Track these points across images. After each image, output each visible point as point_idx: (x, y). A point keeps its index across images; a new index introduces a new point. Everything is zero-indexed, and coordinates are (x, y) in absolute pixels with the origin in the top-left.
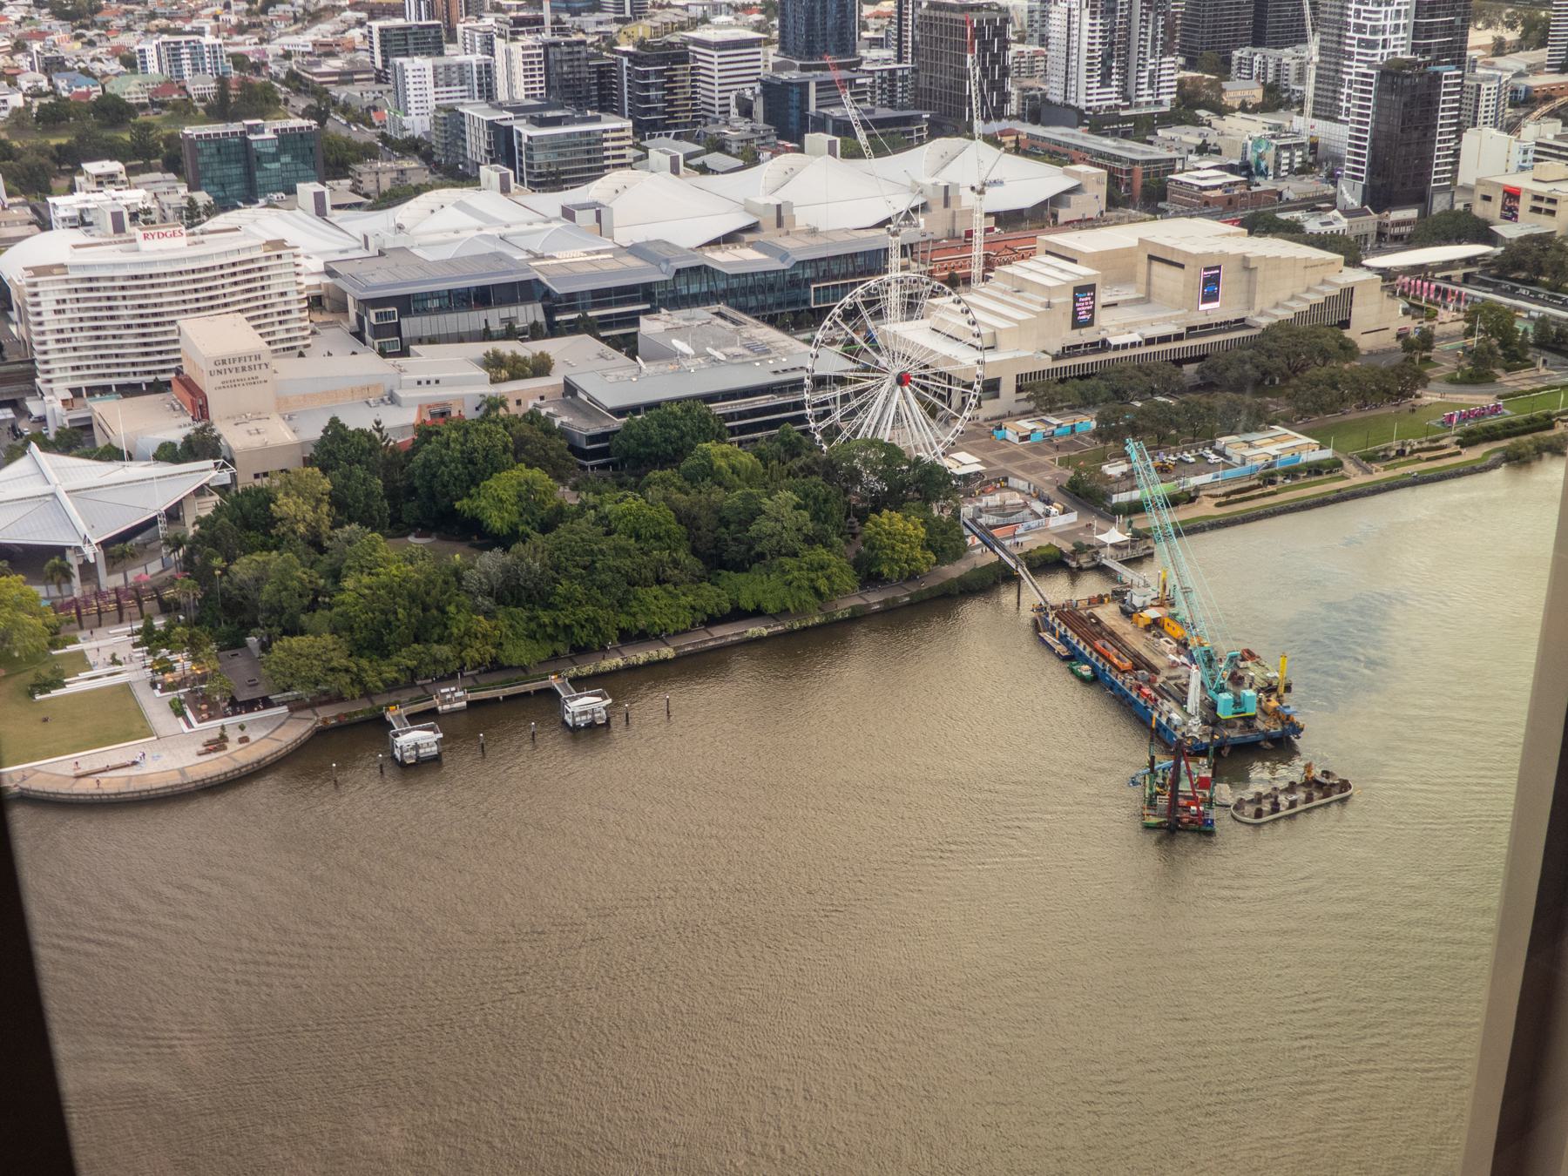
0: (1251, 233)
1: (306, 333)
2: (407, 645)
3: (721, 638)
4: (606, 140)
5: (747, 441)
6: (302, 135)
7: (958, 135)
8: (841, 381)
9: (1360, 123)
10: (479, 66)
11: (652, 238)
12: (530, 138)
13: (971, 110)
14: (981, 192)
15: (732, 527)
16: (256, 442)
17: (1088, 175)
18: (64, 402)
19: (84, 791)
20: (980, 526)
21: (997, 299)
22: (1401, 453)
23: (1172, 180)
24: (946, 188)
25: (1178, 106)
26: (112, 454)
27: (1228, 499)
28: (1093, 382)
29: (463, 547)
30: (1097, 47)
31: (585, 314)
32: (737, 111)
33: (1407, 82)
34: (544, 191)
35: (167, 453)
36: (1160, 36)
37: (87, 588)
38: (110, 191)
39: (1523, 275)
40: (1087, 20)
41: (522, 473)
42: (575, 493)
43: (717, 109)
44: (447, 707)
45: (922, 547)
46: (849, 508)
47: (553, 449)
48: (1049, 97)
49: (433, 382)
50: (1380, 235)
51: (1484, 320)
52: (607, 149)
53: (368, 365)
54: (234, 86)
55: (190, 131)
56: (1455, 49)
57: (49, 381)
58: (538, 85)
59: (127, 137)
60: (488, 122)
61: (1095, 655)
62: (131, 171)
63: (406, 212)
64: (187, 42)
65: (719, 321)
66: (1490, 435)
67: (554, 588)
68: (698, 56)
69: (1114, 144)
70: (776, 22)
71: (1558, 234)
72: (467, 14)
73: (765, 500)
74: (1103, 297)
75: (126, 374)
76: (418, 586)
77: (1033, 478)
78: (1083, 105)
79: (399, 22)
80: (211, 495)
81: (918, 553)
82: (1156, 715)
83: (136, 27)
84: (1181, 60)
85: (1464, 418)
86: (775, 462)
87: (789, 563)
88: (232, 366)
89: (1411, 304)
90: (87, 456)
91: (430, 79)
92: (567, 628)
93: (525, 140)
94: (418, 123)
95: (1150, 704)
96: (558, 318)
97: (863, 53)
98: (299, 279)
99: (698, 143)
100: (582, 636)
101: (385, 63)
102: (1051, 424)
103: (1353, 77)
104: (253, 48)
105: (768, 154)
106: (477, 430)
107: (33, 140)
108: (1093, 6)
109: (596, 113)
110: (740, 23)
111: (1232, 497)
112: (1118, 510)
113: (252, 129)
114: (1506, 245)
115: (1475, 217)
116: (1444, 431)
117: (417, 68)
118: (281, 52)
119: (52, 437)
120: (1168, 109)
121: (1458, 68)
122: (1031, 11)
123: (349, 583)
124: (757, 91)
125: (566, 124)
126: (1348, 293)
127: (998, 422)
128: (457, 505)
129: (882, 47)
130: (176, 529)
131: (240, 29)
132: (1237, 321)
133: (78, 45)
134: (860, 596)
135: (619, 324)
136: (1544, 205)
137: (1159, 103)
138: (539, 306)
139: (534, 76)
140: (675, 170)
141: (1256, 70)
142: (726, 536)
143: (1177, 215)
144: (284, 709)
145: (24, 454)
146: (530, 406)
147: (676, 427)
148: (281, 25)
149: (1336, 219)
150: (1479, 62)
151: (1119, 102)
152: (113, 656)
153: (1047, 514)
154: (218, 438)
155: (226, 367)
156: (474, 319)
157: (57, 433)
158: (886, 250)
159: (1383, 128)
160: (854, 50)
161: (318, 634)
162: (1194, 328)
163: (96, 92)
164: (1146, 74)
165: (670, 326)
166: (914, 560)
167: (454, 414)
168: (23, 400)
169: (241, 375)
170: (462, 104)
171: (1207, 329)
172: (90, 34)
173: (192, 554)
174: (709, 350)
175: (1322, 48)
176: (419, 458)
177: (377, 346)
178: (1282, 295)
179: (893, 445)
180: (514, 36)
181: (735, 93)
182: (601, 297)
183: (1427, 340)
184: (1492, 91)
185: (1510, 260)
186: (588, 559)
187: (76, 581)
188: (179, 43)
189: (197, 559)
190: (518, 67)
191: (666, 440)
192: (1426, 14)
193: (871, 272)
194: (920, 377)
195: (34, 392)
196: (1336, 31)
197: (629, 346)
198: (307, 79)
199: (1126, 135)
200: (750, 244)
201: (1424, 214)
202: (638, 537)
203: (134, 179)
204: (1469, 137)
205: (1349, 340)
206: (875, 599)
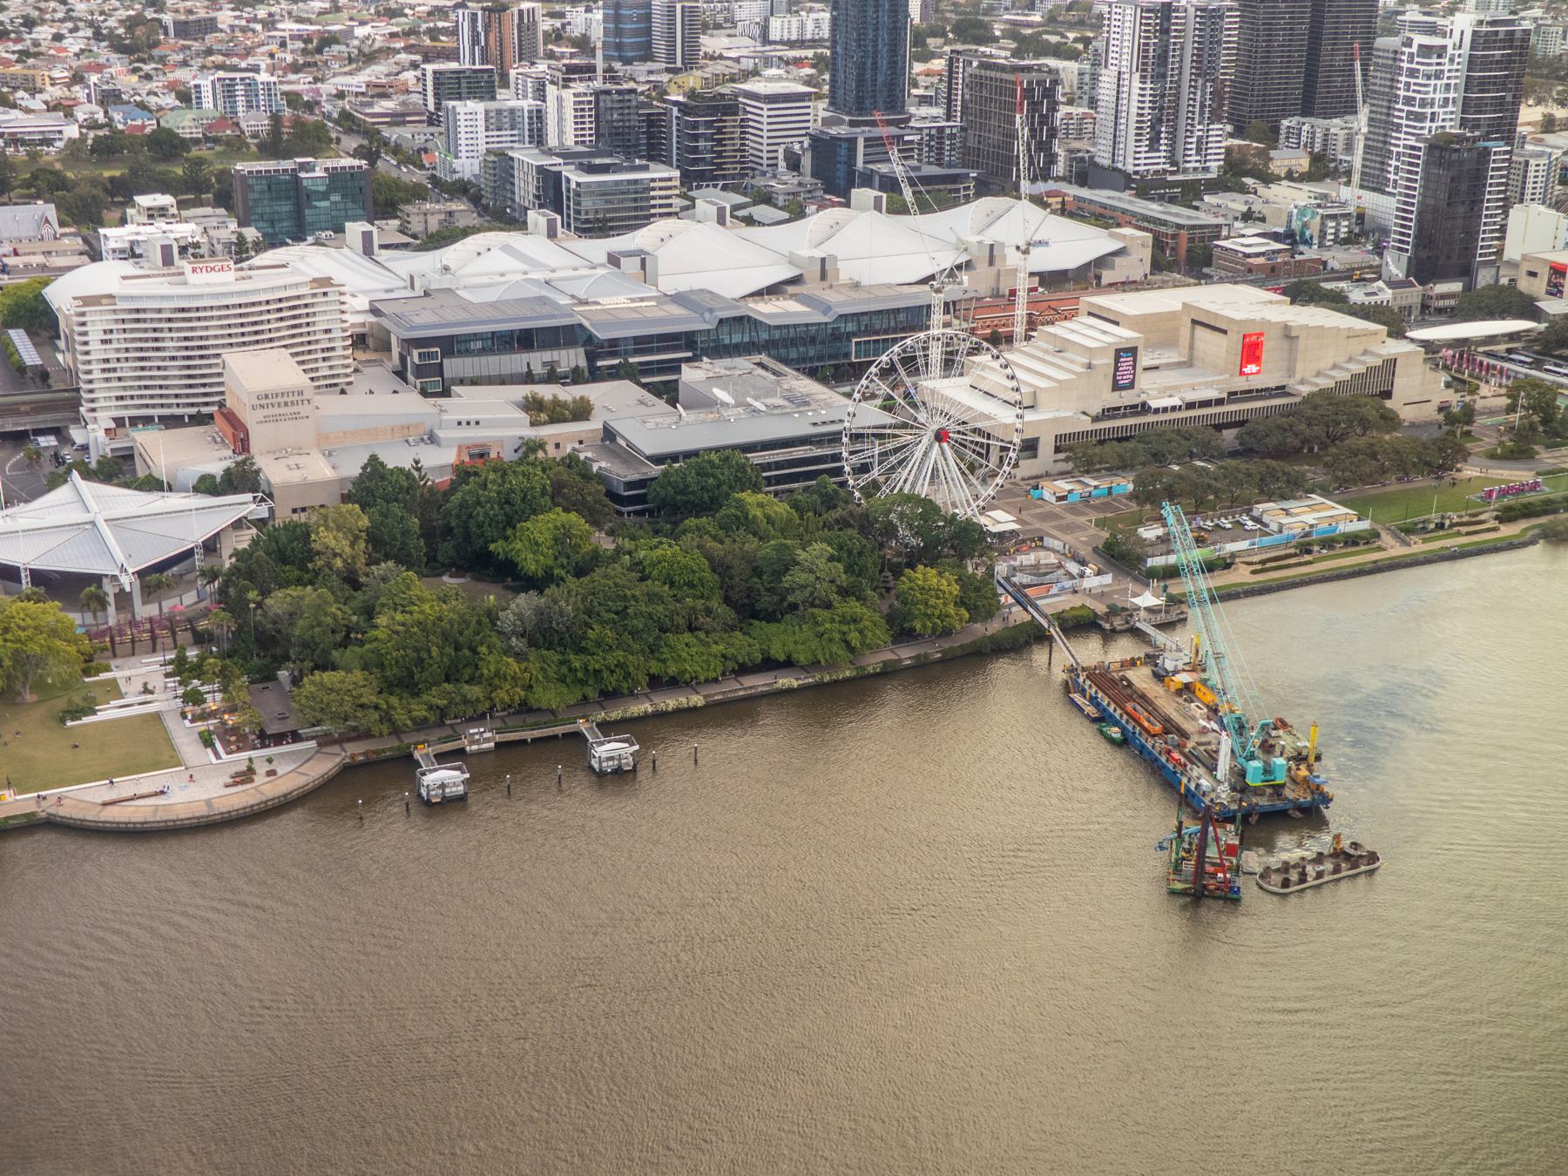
0: (1292, 303)
1: (349, 371)
2: (437, 684)
3: (751, 688)
4: (653, 189)
5: (783, 492)
6: (352, 175)
7: (1005, 195)
9: (1407, 195)
10: (530, 112)
11: (696, 287)
12: (578, 184)
13: (1018, 170)
14: (1026, 252)
15: (765, 577)
16: (295, 477)
17: (1133, 238)
18: (107, 431)
19: (111, 819)
20: (1014, 585)
21: (1039, 359)
22: (1440, 526)
23: (1218, 246)
24: (992, 246)
25: (1226, 173)
26: (153, 484)
27: (1263, 566)
28: (1131, 445)
29: (498, 588)
30: (1147, 111)
31: (626, 360)
32: (784, 164)
33: (1455, 156)
34: (591, 238)
35: (207, 486)
36: (1208, 103)
38: (161, 224)
40: (1136, 84)
41: (558, 517)
42: (612, 539)
43: (765, 162)
44: (475, 747)
45: (956, 603)
46: (883, 564)
47: (590, 494)
48: (1096, 159)
49: (473, 423)
50: (1425, 307)
51: (1528, 396)
52: (654, 198)
53: (410, 404)
54: (287, 124)
56: (1505, 125)
57: (93, 410)
58: (588, 132)
59: (179, 171)
60: (537, 167)
61: (1125, 717)
62: (182, 205)
63: (452, 254)
64: (242, 79)
65: (760, 371)
66: (1528, 512)
67: (585, 633)
68: (748, 109)
69: (1161, 208)
70: (827, 77)
72: (520, 60)
73: (799, 551)
74: (1145, 360)
75: (170, 406)
76: (452, 626)
77: (1068, 538)
78: (1130, 168)
79: (454, 65)
80: (249, 528)
81: (951, 610)
82: (1185, 780)
83: (192, 63)
84: (1229, 128)
85: (1504, 493)
86: (810, 514)
87: (822, 614)
88: (275, 400)
89: (1454, 378)
90: (127, 485)
91: (481, 123)
92: (597, 672)
93: (573, 186)
94: (467, 166)
95: (1179, 769)
96: (599, 364)
97: (912, 110)
98: (344, 317)
99: (745, 195)
100: (611, 681)
101: (438, 106)
102: (1087, 485)
103: (1401, 150)
104: (307, 86)
106: (514, 472)
108: (1143, 70)
109: (644, 162)
110: (791, 77)
111: (1268, 565)
112: (1153, 574)
113: (303, 167)
114: (1549, 322)
115: (1521, 293)
116: (1482, 506)
117: (469, 110)
118: (334, 92)
119: (93, 465)
120: (1215, 176)
121: (1507, 144)
122: (1081, 74)
123: (382, 620)
124: (806, 145)
126: (1391, 364)
127: (1035, 481)
128: (492, 547)
129: (931, 105)
130: (212, 561)
131: (295, 68)
132: (1277, 388)
133: (135, 78)
134: (892, 651)
137: (1206, 169)
138: (581, 351)
139: (584, 123)
140: (721, 221)
141: (1303, 139)
142: (759, 586)
143: (1221, 280)
144: (313, 744)
145: (66, 481)
146: (569, 450)
147: (713, 475)
149: (1381, 290)
150: (1529, 138)
151: (1167, 167)
152: (145, 684)
153: (1082, 575)
154: (257, 472)
155: (269, 401)
156: (516, 362)
157: (99, 462)
158: (929, 306)
159: (1432, 202)
160: (903, 107)
161: (349, 671)
162: (1235, 393)
164: (1194, 140)
165: (711, 375)
166: (948, 616)
167: (493, 455)
168: (67, 427)
169: (283, 410)
170: (512, 148)
171: (1249, 395)
172: (147, 68)
173: (228, 587)
174: (749, 400)
175: (1371, 119)
176: (456, 498)
177: (418, 385)
178: (1325, 364)
179: (930, 501)
180: (566, 84)
181: (783, 146)
182: (643, 344)
183: (1468, 414)
184: (1541, 168)
185: (1555, 337)
186: (620, 605)
187: (111, 610)
188: (234, 79)
189: (232, 591)
190: (569, 114)
191: (702, 488)
192: (1476, 89)
193: (914, 328)
194: (959, 432)
195: (78, 420)
196: (1385, 104)
197: (669, 393)
198: (360, 120)
199: (1172, 200)
200: (793, 296)
201: (1468, 288)
202: (672, 584)
203: (184, 213)
204: (1516, 212)
205: (1391, 411)
206: (906, 654)
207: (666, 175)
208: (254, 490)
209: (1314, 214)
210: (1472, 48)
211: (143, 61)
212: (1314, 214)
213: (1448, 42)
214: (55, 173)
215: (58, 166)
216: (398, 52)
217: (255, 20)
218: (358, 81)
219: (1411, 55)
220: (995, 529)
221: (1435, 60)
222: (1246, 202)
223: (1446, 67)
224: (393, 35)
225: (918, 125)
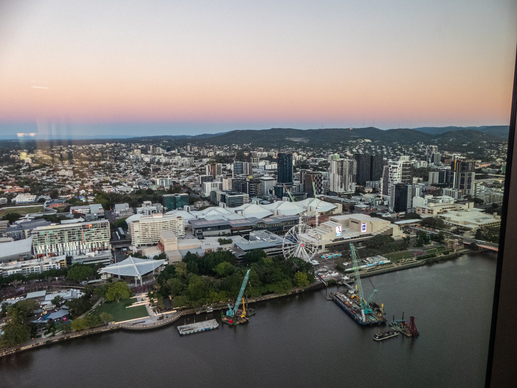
0: (371, 217)
2: (201, 298)
8: (290, 245)
12: (229, 197)
20: (318, 275)
26: (145, 258)
27: (369, 270)
28: (341, 246)
30: (340, 181)
35: (156, 258)
37: (138, 285)
38: (148, 206)
39: (427, 225)
40: (337, 176)
41: (225, 263)
43: (265, 192)
44: (209, 311)
50: (397, 217)
51: (420, 234)
55: (165, 195)
57: (134, 243)
63: (204, 211)
65: (265, 233)
66: (424, 258)
70: (277, 176)
71: (434, 217)
75: (149, 242)
78: (337, 192)
79: (205, 175)
82: (356, 317)
84: (356, 183)
87: (279, 283)
88: (170, 241)
90: (140, 258)
92: (233, 295)
93: (228, 198)
94: (207, 194)
95: (354, 314)
99: (261, 198)
101: (202, 183)
102: (332, 255)
105: (275, 201)
107: (135, 196)
112: (347, 272)
113: (176, 195)
115: (417, 214)
119: (134, 254)
120: (354, 193)
123: (190, 285)
125: (236, 195)
126: (392, 229)
127: (322, 254)
128: (212, 269)
131: (175, 177)
133: (144, 180)
136: (430, 212)
137: (352, 192)
140: (257, 204)
144: (176, 311)
145: (128, 257)
146: (227, 249)
148: (182, 176)
149: (389, 214)
154: (166, 255)
156: (217, 232)
162: (361, 235)
163: (147, 188)
167: (212, 251)
168: (129, 247)
169: (171, 242)
171: (363, 236)
172: (147, 178)
174: (263, 239)
175: (383, 181)
176: (205, 260)
178: (379, 229)
180: (226, 178)
183: (408, 238)
187: (136, 283)
188: (163, 179)
197: (247, 238)
201: (406, 213)
203: (153, 204)
205: (393, 238)
207: (246, 195)
208: (165, 258)
210: (403, 167)
211: (146, 176)
213: (398, 166)
214: (129, 197)
215: (129, 196)
216: (194, 173)
217: (167, 168)
218: (187, 179)
219: (391, 169)
220: (314, 264)
221: (395, 169)
222: (360, 198)
223: (398, 171)
224: (194, 170)
225: (295, 184)
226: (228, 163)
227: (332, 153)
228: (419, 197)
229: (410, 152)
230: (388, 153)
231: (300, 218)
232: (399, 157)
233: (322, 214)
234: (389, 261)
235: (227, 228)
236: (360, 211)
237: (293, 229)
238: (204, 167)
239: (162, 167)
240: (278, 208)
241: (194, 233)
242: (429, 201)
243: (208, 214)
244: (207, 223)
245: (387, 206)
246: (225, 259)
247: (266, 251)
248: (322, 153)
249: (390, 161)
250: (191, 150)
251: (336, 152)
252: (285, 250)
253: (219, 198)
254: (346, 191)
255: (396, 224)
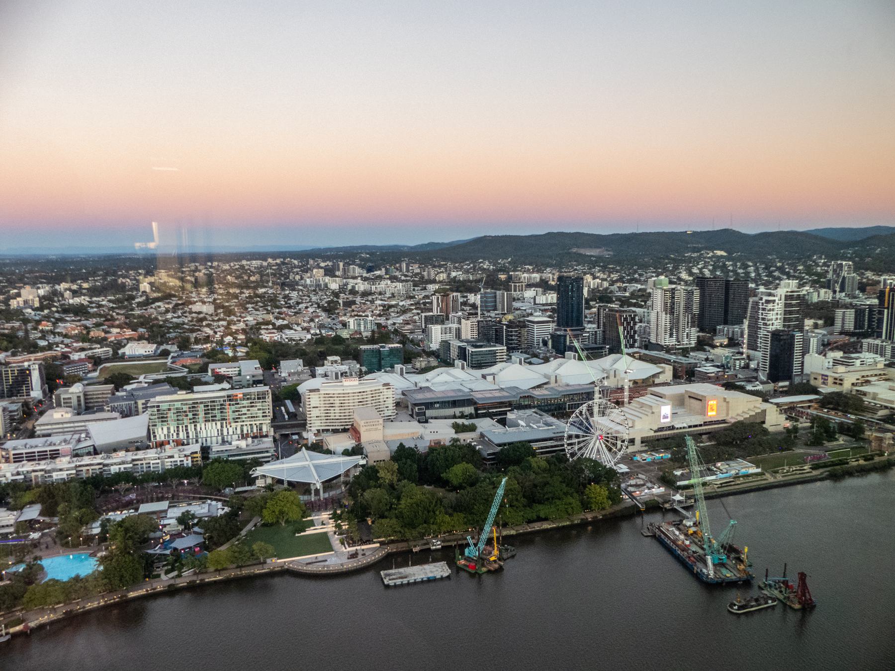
8: (577, 436)
20: (628, 491)
26: (329, 452)
27: (722, 485)
28: (669, 440)
35: (346, 453)
38: (335, 365)
40: (664, 315)
50: (775, 391)
51: (818, 423)
55: (363, 347)
62: (342, 360)
63: (430, 375)
65: (535, 414)
66: (825, 466)
71: (844, 392)
78: (663, 344)
79: (431, 314)
82: (695, 568)
84: (698, 329)
87: (558, 502)
90: (320, 452)
92: (478, 521)
94: (434, 346)
107: (312, 348)
113: (382, 347)
119: (309, 445)
123: (403, 502)
126: (764, 411)
127: (634, 454)
128: (442, 475)
130: (347, 479)
131: (380, 315)
133: (329, 320)
135: (500, 415)
136: (838, 381)
140: (520, 363)
143: (698, 382)
144: (378, 545)
148: (393, 314)
154: (362, 448)
156: (450, 411)
159: (774, 353)
163: (333, 334)
167: (442, 443)
169: (372, 427)
172: (333, 316)
175: (749, 326)
176: (429, 458)
178: (740, 412)
180: (468, 319)
183: (795, 429)
186: (486, 497)
187: (313, 495)
197: (503, 422)
201: (791, 384)
203: (343, 362)
204: (807, 357)
208: (362, 454)
209: (731, 359)
212: (731, 359)
213: (776, 299)
214: (303, 350)
216: (413, 310)
217: (368, 301)
218: (400, 320)
221: (772, 305)
223: (776, 307)
226: (471, 292)
227: (654, 275)
228: (816, 355)
229: (800, 273)
230: (758, 275)
231: (597, 389)
232: (777, 282)
233: (635, 382)
234: (759, 470)
235: (468, 405)
236: (705, 378)
237: (584, 408)
238: (429, 299)
239: (358, 299)
240: (557, 372)
241: (410, 413)
242: (836, 362)
243: (433, 381)
244: (433, 396)
245: (756, 370)
246: (464, 458)
247: (535, 446)
248: (636, 276)
249: (762, 289)
250: (408, 270)
251: (661, 274)
252: (569, 445)
253: (454, 353)
254: (679, 342)
255: (772, 403)
